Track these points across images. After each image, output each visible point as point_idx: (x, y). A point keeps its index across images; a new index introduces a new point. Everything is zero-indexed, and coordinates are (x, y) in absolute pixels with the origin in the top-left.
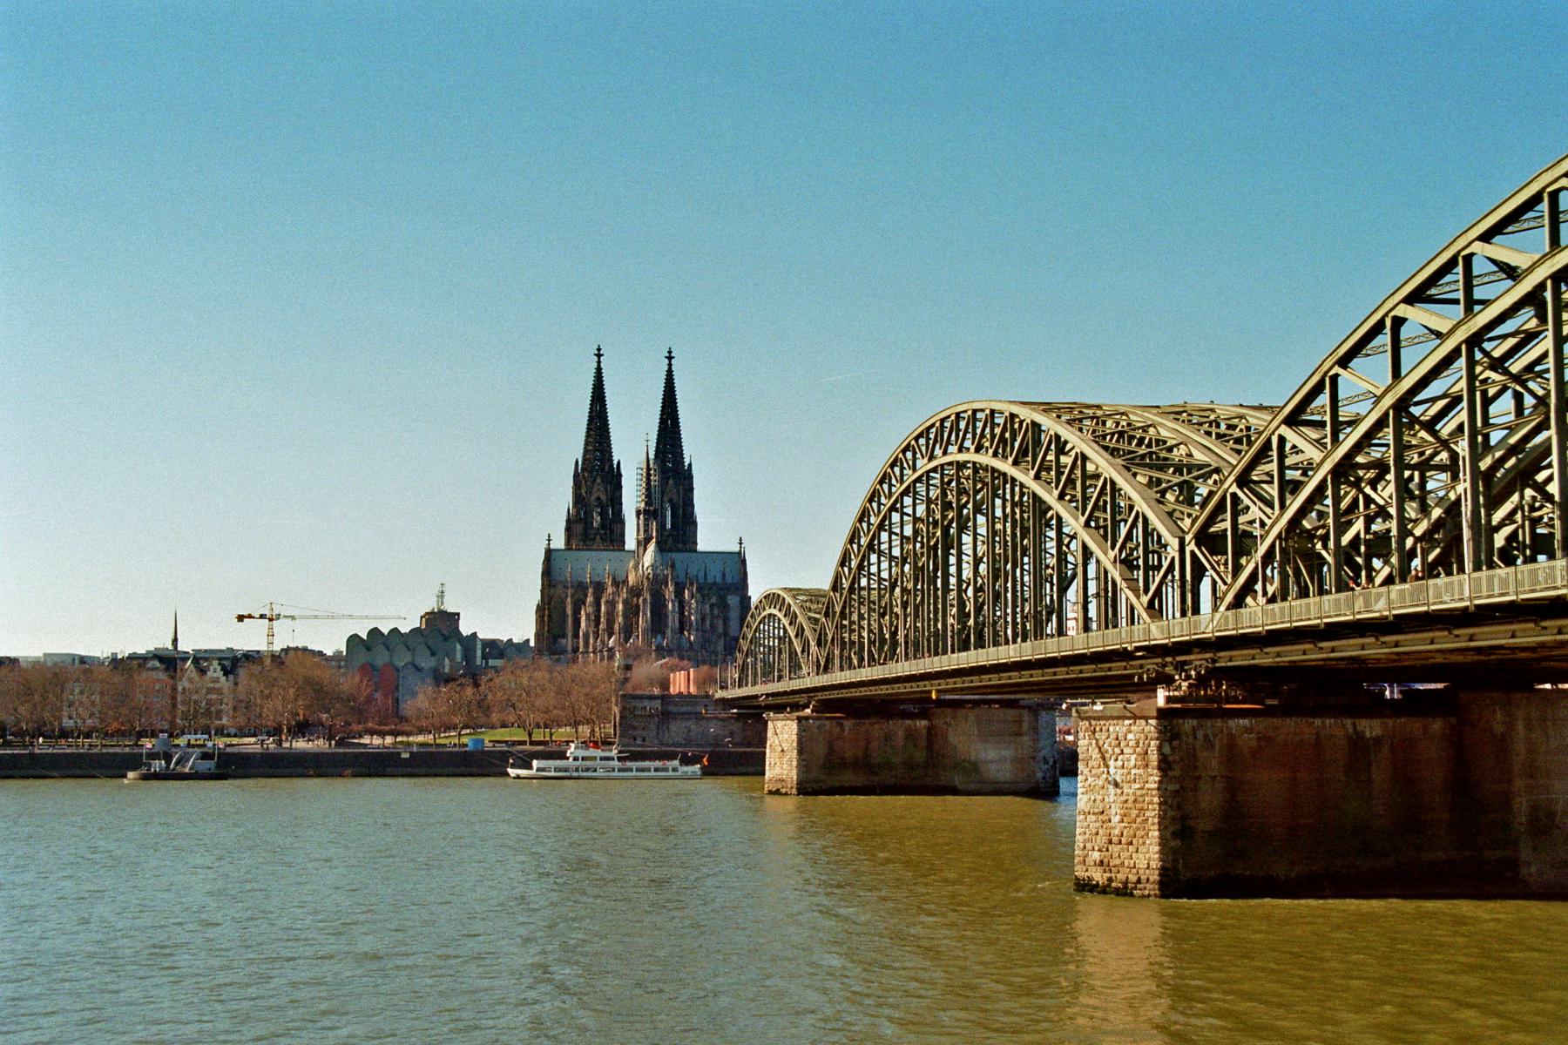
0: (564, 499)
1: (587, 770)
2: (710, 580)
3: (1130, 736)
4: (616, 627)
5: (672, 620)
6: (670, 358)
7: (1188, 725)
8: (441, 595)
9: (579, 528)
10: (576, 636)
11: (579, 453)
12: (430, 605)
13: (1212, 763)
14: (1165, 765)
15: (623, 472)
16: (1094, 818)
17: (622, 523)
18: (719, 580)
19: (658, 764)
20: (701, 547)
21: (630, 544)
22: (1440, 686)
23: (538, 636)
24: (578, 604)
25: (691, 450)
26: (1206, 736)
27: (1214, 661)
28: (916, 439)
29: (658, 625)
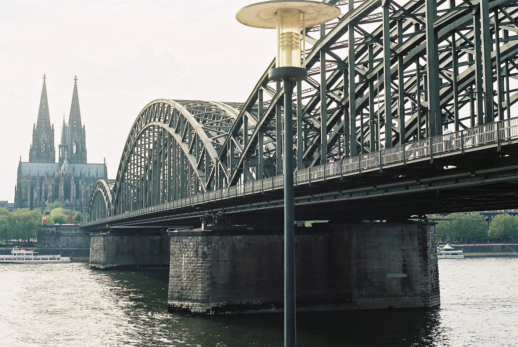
0: (29, 141)
1: (20, 259)
2: (91, 176)
3: (191, 244)
4: (49, 195)
5: (73, 193)
6: (76, 80)
7: (215, 238)
9: (35, 153)
11: (35, 120)
13: (225, 255)
14: (205, 255)
15: (54, 128)
16: (176, 279)
18: (95, 176)
19: (51, 256)
20: (88, 162)
21: (57, 161)
22: (327, 221)
25: (84, 121)
26: (223, 243)
27: (225, 211)
28: (142, 115)
29: (67, 195)
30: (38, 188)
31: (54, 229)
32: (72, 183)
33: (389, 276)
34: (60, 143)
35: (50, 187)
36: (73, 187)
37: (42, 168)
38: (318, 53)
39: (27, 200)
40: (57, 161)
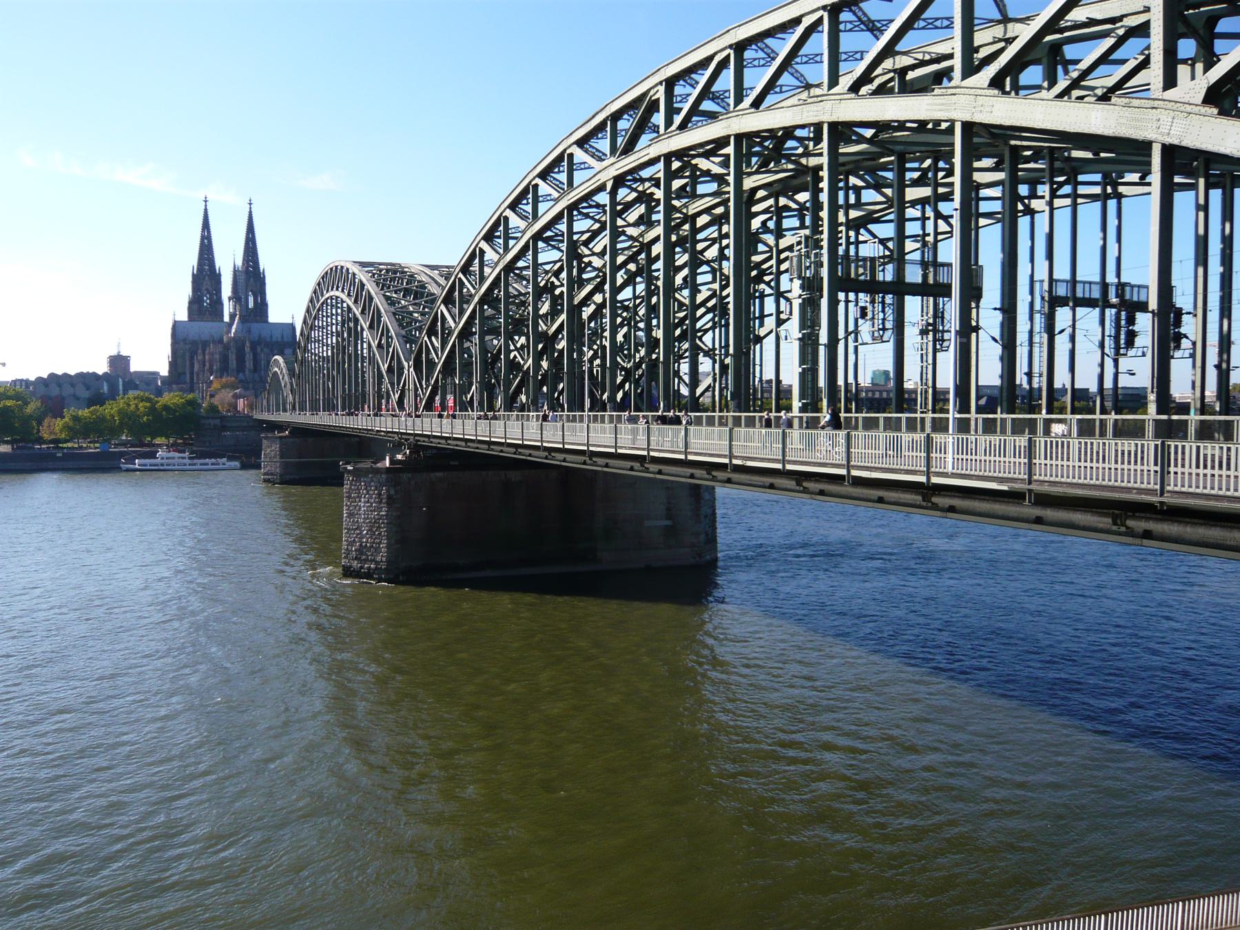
0: (186, 291)
2: (274, 339)
5: (249, 364)
8: (119, 346)
9: (195, 307)
10: (192, 373)
12: (114, 353)
17: (221, 304)
19: (213, 460)
21: (226, 319)
23: (170, 372)
24: (193, 354)
25: (264, 262)
29: (241, 367)
30: (200, 357)
31: (218, 422)
32: (247, 349)
33: (647, 523)
34: (230, 294)
35: (217, 356)
36: (249, 357)
37: (206, 328)
38: (528, 242)
39: (184, 374)
40: (226, 319)
